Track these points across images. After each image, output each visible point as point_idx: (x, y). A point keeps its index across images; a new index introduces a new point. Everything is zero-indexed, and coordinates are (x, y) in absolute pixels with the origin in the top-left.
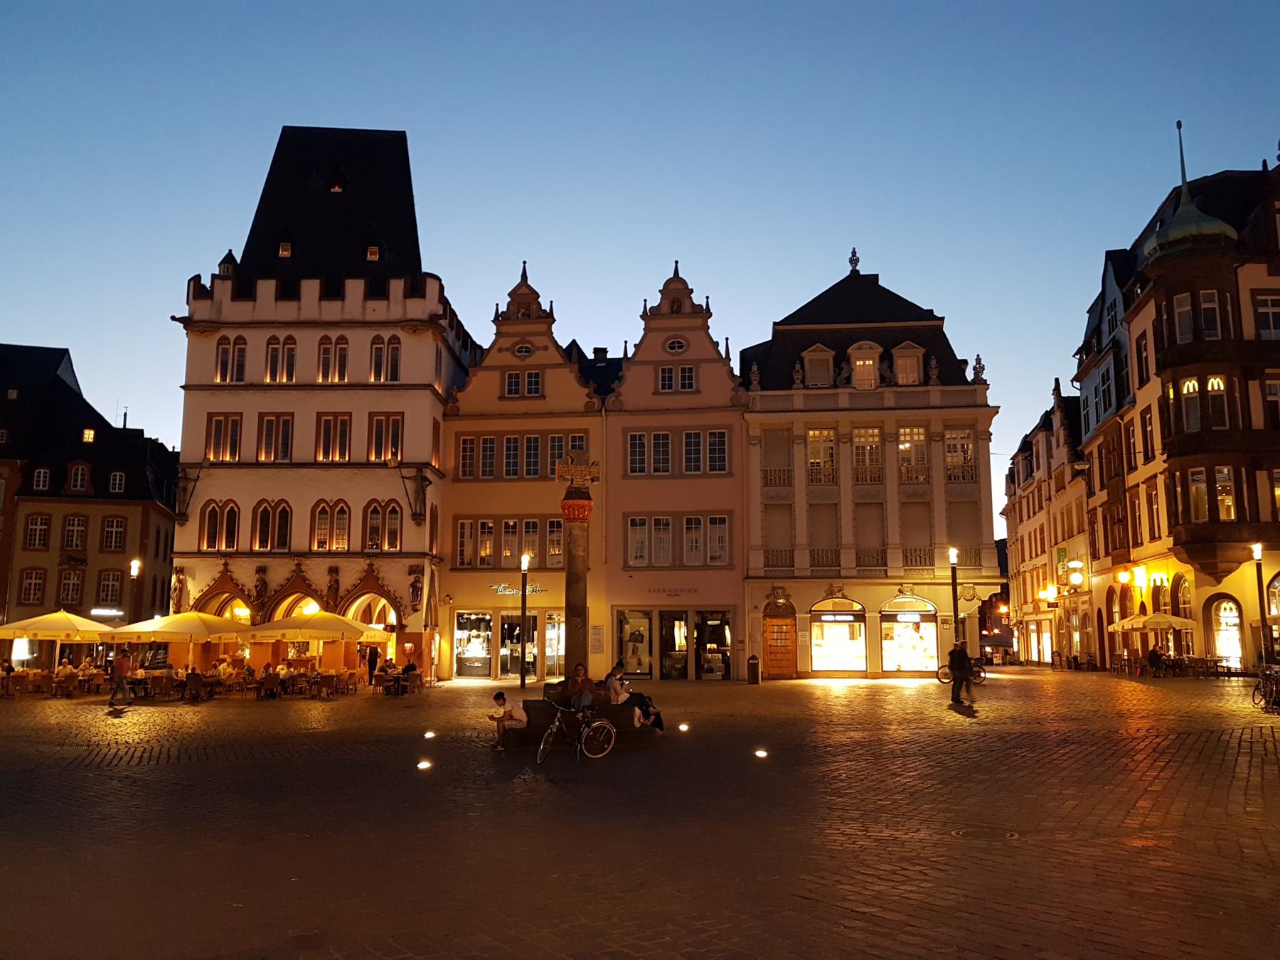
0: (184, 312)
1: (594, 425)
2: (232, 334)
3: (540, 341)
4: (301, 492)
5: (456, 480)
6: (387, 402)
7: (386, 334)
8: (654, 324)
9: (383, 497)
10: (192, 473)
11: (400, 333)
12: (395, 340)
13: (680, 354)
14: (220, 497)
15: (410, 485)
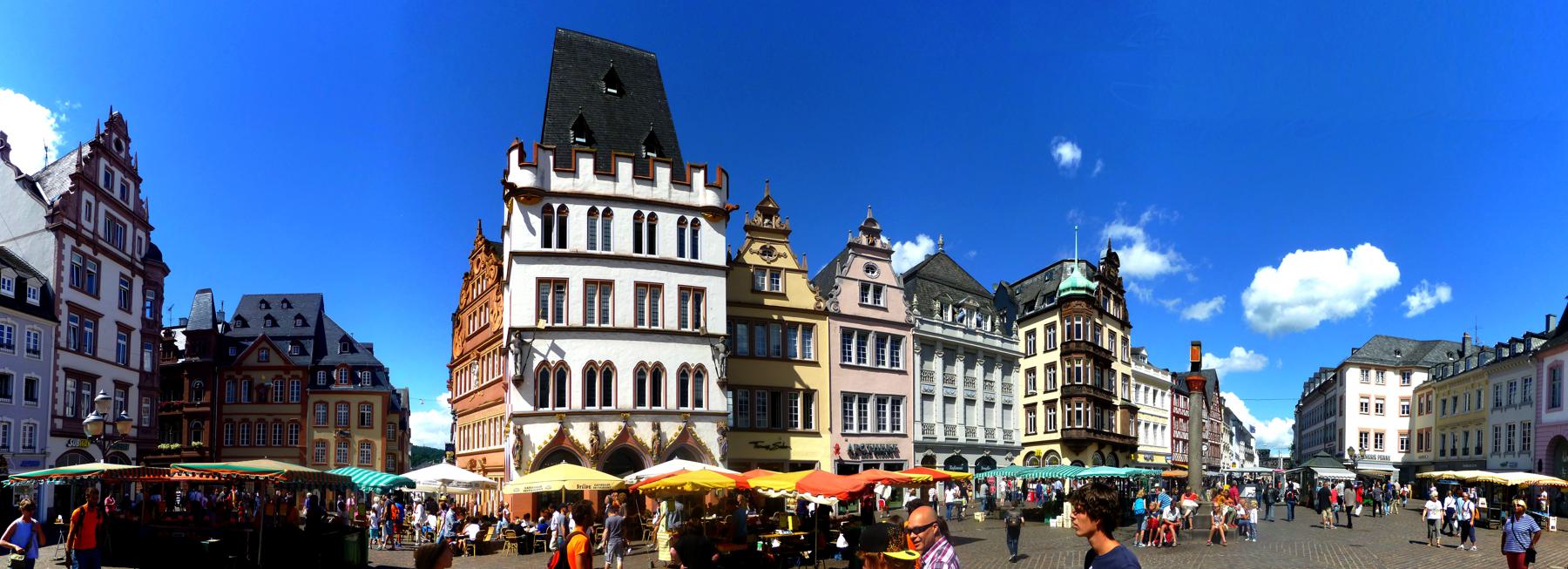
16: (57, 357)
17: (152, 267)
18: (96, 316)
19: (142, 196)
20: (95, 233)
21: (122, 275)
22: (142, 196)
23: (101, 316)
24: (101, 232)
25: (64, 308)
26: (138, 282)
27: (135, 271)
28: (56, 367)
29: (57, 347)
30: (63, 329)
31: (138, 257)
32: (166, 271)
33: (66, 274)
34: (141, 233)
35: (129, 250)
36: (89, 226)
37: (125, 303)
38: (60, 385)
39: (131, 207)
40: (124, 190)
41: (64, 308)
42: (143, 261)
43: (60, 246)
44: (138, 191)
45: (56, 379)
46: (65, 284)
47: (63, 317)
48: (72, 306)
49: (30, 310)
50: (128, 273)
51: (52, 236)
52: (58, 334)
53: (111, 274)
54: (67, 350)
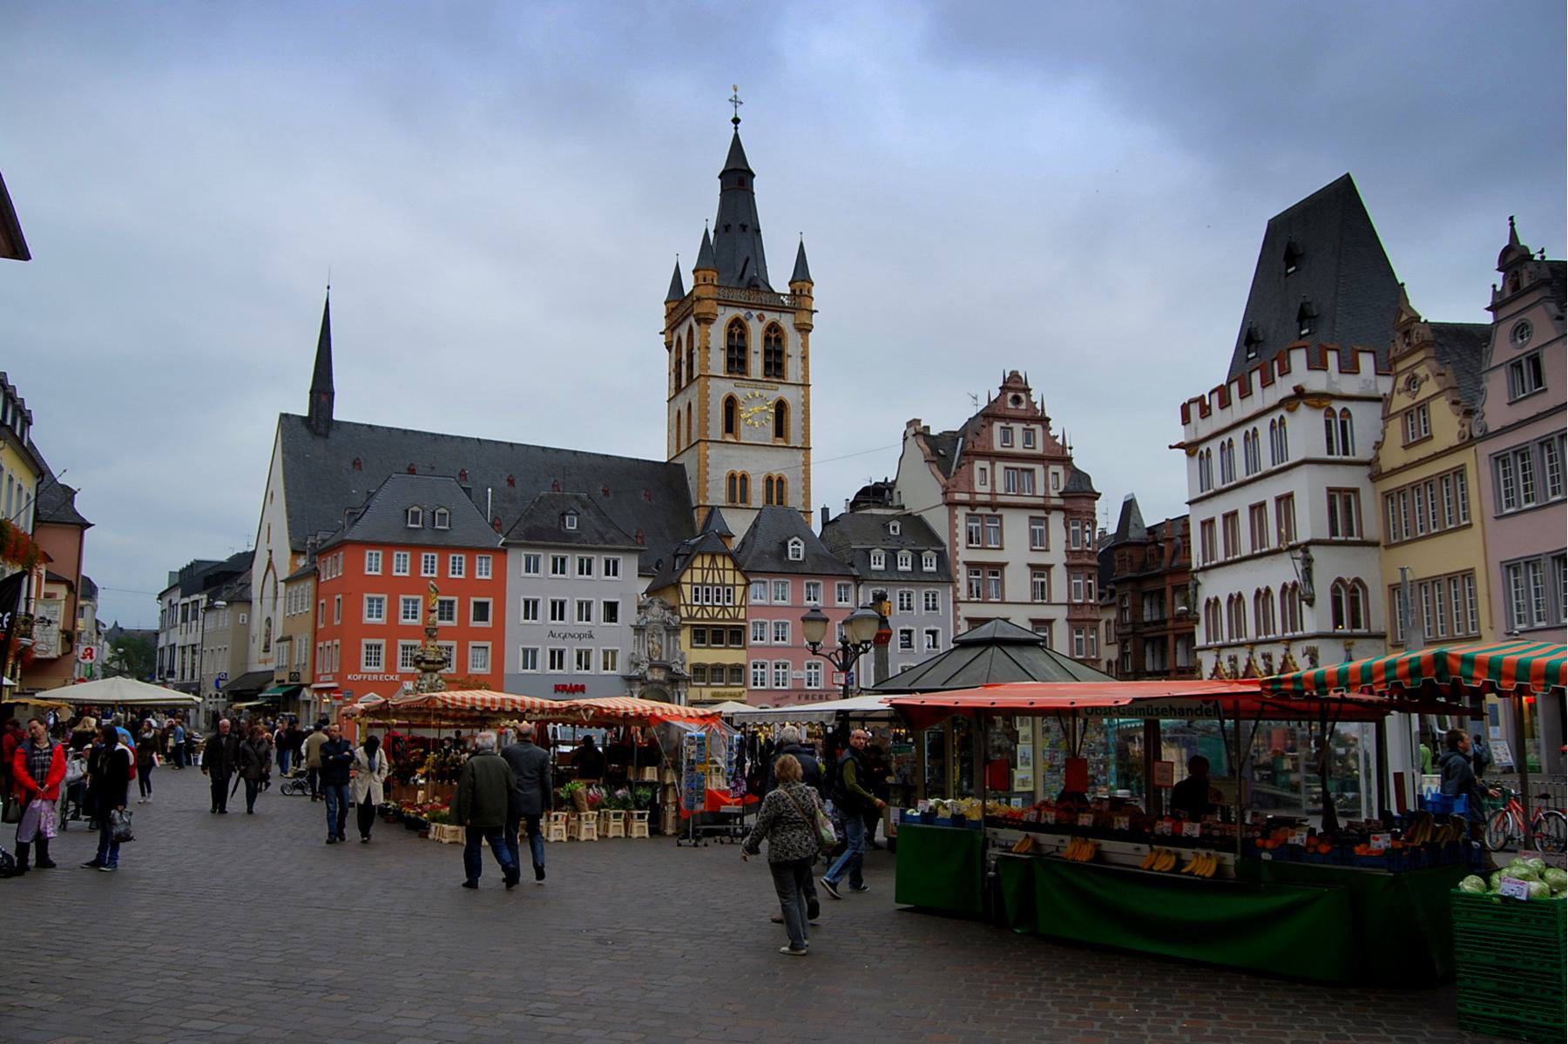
0: (1180, 434)
1: (1466, 458)
2: (1203, 448)
3: (1421, 371)
4: (1245, 581)
5: (1387, 547)
6: (1278, 486)
7: (1276, 416)
8: (1503, 314)
9: (1289, 582)
10: (1200, 577)
11: (1282, 412)
12: (1282, 418)
13: (1522, 347)
14: (1212, 597)
15: (1300, 568)
16: (956, 609)
17: (1080, 493)
18: (1002, 566)
19: (1052, 433)
20: (993, 494)
22: (1052, 433)
24: (1000, 488)
26: (1056, 521)
27: (1048, 509)
28: (956, 618)
30: (963, 586)
31: (1053, 493)
32: (1097, 496)
33: (962, 539)
34: (1053, 468)
35: (1040, 491)
36: (987, 489)
37: (1039, 540)
39: (1039, 450)
40: (1029, 437)
42: (1062, 495)
43: (952, 517)
44: (1047, 428)
47: (962, 575)
49: (931, 580)
50: (1042, 514)
51: (945, 509)
52: (956, 591)
53: (1016, 527)
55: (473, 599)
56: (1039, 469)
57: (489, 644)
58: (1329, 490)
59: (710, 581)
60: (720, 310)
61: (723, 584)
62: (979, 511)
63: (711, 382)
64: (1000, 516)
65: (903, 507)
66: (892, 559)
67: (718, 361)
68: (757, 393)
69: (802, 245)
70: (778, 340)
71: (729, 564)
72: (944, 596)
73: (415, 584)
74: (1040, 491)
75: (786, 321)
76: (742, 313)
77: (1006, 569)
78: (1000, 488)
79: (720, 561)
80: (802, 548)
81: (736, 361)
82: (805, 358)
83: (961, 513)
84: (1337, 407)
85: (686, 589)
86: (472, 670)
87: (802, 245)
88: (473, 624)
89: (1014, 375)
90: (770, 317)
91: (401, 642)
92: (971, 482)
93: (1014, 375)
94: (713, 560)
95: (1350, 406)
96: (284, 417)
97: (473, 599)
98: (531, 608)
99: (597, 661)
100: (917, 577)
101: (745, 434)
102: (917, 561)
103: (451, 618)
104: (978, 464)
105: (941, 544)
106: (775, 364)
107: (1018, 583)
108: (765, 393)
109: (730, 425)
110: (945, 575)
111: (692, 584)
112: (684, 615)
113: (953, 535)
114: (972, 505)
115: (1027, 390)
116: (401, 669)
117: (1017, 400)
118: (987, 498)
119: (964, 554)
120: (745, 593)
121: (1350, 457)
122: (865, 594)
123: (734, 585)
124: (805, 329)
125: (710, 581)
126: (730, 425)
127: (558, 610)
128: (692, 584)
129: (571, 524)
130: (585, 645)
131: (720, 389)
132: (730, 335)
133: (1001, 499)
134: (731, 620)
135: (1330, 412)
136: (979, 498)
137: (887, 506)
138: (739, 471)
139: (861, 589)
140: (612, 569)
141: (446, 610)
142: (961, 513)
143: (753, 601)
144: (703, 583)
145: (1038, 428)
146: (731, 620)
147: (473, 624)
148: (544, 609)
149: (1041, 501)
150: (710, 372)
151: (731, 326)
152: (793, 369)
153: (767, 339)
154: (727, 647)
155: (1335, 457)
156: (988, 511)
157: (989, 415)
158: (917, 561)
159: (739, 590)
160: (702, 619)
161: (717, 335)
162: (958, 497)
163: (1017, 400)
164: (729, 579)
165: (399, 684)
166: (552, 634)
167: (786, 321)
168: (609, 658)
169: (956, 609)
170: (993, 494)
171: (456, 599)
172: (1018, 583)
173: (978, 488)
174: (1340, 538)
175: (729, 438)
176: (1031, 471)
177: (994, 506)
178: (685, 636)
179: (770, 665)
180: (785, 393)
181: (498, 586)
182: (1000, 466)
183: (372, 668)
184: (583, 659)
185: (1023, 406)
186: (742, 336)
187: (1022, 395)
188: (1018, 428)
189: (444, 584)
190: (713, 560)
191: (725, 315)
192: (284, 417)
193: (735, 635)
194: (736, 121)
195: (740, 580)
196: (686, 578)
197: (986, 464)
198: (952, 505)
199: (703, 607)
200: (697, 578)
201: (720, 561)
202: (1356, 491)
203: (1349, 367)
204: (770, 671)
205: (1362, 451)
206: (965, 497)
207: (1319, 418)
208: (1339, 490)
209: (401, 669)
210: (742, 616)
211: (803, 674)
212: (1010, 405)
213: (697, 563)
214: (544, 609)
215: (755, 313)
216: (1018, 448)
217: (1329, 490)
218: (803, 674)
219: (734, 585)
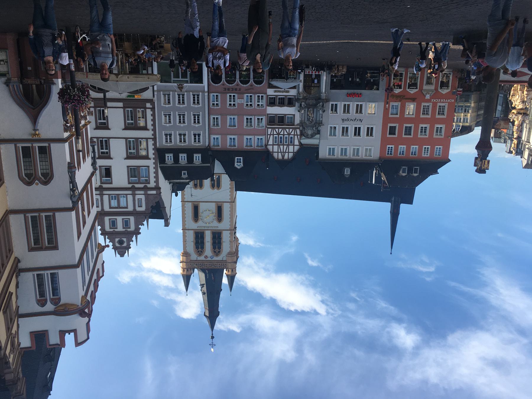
16: (154, 135)
20: (134, 195)
21: (111, 183)
23: (125, 159)
25: (151, 155)
29: (154, 139)
33: (152, 170)
35: (106, 198)
36: (137, 197)
38: (150, 123)
39: (107, 219)
41: (151, 155)
43: (157, 182)
45: (154, 125)
46: (152, 166)
47: (151, 152)
48: (147, 157)
50: (105, 186)
51: (160, 186)
54: (147, 139)
55: (396, 136)
56: (107, 208)
57: (390, 116)
58: (56, 248)
59: (285, 147)
60: (225, 259)
61: (278, 145)
62: (142, 186)
63: (228, 227)
64: (129, 183)
65: (170, 183)
66: (190, 159)
67: (226, 237)
68: (208, 225)
69: (187, 290)
70: (197, 248)
71: (275, 155)
72: (162, 142)
73: (421, 143)
74: (106, 198)
75: (194, 256)
76: (215, 258)
77: (125, 156)
78: (130, 198)
79: (280, 157)
80: (236, 164)
81: (217, 237)
82: (185, 241)
83: (152, 184)
84: (49, 307)
85: (296, 142)
86: (398, 104)
87: (187, 290)
88: (397, 125)
89: (122, 255)
90: (202, 258)
91: (429, 116)
92: (146, 199)
93: (122, 255)
94: (283, 156)
95: (39, 309)
96: (410, 202)
97: (396, 136)
98: (370, 132)
99: (340, 109)
100: (176, 152)
101: (213, 207)
102: (176, 159)
103: (406, 127)
104: (143, 209)
105: (161, 167)
106: (199, 237)
107: (118, 149)
108: (204, 225)
109: (220, 210)
110: (161, 153)
111: (294, 145)
112: (298, 131)
113: (156, 173)
114: (145, 189)
115: (115, 248)
116: (430, 104)
117: (121, 242)
118: (137, 192)
119: (150, 163)
120: (268, 141)
121: (36, 273)
122: (204, 141)
123: (273, 145)
124: (185, 254)
125: (285, 147)
126: (220, 210)
127: (357, 132)
128: (294, 145)
129: (347, 171)
130: (346, 116)
131: (225, 225)
132: (220, 248)
133: (130, 192)
134: (275, 128)
135: (56, 301)
136: (142, 192)
137: (177, 183)
138: (216, 190)
139: (207, 144)
140: (332, 151)
141: (408, 131)
142: (152, 184)
143: (263, 137)
144: (288, 145)
145: (107, 228)
146: (275, 128)
147: (397, 125)
148: (364, 132)
149: (105, 192)
150: (229, 232)
151: (219, 252)
152: (191, 236)
153: (203, 248)
154: (276, 115)
155: (49, 272)
156: (137, 186)
157: (137, 232)
158: (176, 159)
159: (271, 142)
160: (289, 128)
161: (226, 247)
162: (154, 192)
163: (121, 242)
164: (276, 148)
165: (432, 97)
166: (361, 120)
167: (194, 256)
168: (334, 108)
169: (154, 135)
170: (134, 195)
171: (404, 136)
172: (118, 149)
173: (143, 197)
174: (43, 215)
175: (220, 204)
176: (110, 208)
177: (133, 189)
178: (297, 121)
179: (255, 106)
180: (195, 226)
181: (384, 141)
182: (130, 208)
183: (442, 104)
184: (347, 109)
185: (117, 240)
186: (214, 248)
187: (117, 245)
188: (120, 228)
189: (409, 143)
190: (283, 156)
191: (222, 256)
192: (410, 202)
193: (273, 120)
194: (213, 337)
195: (270, 148)
196: (297, 148)
197: (138, 209)
198: (157, 188)
199: (289, 134)
200: (291, 148)
201: (280, 157)
202: (31, 249)
203: (39, 337)
204: (255, 102)
205: (28, 280)
206: (150, 192)
207: (65, 298)
208: (47, 249)
209: (430, 104)
210: (270, 130)
211: (238, 101)
212: (125, 240)
213: (291, 155)
214: (364, 132)
215: (209, 259)
216: (119, 220)
217: (56, 248)
218: (238, 101)
219: (273, 145)
